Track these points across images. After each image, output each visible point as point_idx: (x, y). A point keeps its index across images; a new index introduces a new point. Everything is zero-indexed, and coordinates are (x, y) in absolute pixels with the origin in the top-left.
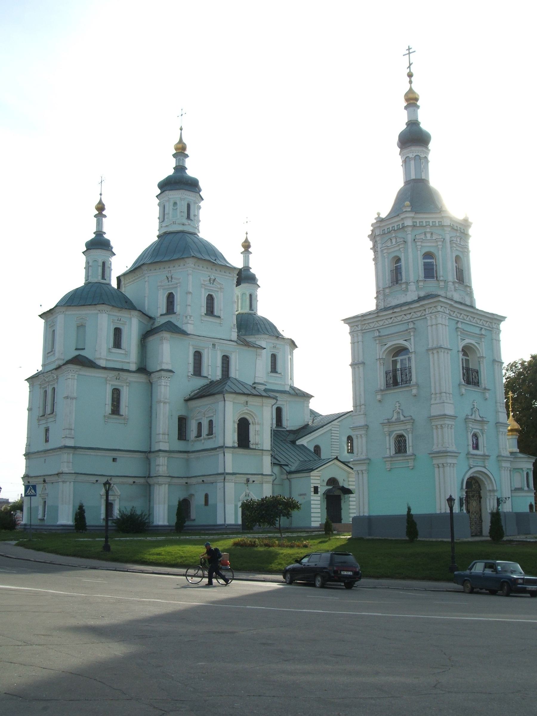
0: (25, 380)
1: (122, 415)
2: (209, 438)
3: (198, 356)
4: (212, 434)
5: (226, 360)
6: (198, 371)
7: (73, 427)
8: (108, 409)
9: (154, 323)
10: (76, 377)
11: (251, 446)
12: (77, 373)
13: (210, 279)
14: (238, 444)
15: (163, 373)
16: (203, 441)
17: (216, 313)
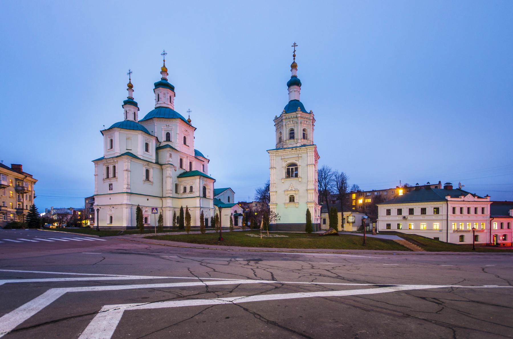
0: (92, 161)
1: (150, 181)
2: (191, 193)
3: (181, 160)
4: (192, 192)
5: (191, 163)
6: (181, 166)
7: (129, 184)
8: (145, 178)
9: (160, 144)
10: (130, 162)
11: (207, 197)
12: (130, 160)
13: (185, 130)
14: (203, 196)
15: (168, 165)
16: (187, 194)
17: (187, 144)
